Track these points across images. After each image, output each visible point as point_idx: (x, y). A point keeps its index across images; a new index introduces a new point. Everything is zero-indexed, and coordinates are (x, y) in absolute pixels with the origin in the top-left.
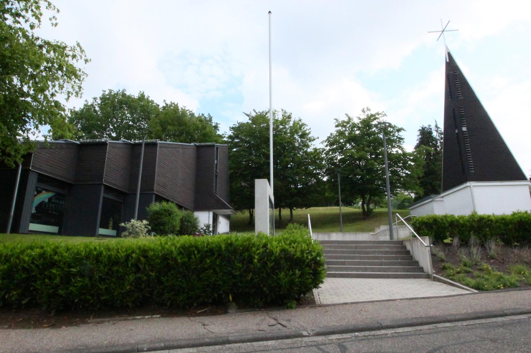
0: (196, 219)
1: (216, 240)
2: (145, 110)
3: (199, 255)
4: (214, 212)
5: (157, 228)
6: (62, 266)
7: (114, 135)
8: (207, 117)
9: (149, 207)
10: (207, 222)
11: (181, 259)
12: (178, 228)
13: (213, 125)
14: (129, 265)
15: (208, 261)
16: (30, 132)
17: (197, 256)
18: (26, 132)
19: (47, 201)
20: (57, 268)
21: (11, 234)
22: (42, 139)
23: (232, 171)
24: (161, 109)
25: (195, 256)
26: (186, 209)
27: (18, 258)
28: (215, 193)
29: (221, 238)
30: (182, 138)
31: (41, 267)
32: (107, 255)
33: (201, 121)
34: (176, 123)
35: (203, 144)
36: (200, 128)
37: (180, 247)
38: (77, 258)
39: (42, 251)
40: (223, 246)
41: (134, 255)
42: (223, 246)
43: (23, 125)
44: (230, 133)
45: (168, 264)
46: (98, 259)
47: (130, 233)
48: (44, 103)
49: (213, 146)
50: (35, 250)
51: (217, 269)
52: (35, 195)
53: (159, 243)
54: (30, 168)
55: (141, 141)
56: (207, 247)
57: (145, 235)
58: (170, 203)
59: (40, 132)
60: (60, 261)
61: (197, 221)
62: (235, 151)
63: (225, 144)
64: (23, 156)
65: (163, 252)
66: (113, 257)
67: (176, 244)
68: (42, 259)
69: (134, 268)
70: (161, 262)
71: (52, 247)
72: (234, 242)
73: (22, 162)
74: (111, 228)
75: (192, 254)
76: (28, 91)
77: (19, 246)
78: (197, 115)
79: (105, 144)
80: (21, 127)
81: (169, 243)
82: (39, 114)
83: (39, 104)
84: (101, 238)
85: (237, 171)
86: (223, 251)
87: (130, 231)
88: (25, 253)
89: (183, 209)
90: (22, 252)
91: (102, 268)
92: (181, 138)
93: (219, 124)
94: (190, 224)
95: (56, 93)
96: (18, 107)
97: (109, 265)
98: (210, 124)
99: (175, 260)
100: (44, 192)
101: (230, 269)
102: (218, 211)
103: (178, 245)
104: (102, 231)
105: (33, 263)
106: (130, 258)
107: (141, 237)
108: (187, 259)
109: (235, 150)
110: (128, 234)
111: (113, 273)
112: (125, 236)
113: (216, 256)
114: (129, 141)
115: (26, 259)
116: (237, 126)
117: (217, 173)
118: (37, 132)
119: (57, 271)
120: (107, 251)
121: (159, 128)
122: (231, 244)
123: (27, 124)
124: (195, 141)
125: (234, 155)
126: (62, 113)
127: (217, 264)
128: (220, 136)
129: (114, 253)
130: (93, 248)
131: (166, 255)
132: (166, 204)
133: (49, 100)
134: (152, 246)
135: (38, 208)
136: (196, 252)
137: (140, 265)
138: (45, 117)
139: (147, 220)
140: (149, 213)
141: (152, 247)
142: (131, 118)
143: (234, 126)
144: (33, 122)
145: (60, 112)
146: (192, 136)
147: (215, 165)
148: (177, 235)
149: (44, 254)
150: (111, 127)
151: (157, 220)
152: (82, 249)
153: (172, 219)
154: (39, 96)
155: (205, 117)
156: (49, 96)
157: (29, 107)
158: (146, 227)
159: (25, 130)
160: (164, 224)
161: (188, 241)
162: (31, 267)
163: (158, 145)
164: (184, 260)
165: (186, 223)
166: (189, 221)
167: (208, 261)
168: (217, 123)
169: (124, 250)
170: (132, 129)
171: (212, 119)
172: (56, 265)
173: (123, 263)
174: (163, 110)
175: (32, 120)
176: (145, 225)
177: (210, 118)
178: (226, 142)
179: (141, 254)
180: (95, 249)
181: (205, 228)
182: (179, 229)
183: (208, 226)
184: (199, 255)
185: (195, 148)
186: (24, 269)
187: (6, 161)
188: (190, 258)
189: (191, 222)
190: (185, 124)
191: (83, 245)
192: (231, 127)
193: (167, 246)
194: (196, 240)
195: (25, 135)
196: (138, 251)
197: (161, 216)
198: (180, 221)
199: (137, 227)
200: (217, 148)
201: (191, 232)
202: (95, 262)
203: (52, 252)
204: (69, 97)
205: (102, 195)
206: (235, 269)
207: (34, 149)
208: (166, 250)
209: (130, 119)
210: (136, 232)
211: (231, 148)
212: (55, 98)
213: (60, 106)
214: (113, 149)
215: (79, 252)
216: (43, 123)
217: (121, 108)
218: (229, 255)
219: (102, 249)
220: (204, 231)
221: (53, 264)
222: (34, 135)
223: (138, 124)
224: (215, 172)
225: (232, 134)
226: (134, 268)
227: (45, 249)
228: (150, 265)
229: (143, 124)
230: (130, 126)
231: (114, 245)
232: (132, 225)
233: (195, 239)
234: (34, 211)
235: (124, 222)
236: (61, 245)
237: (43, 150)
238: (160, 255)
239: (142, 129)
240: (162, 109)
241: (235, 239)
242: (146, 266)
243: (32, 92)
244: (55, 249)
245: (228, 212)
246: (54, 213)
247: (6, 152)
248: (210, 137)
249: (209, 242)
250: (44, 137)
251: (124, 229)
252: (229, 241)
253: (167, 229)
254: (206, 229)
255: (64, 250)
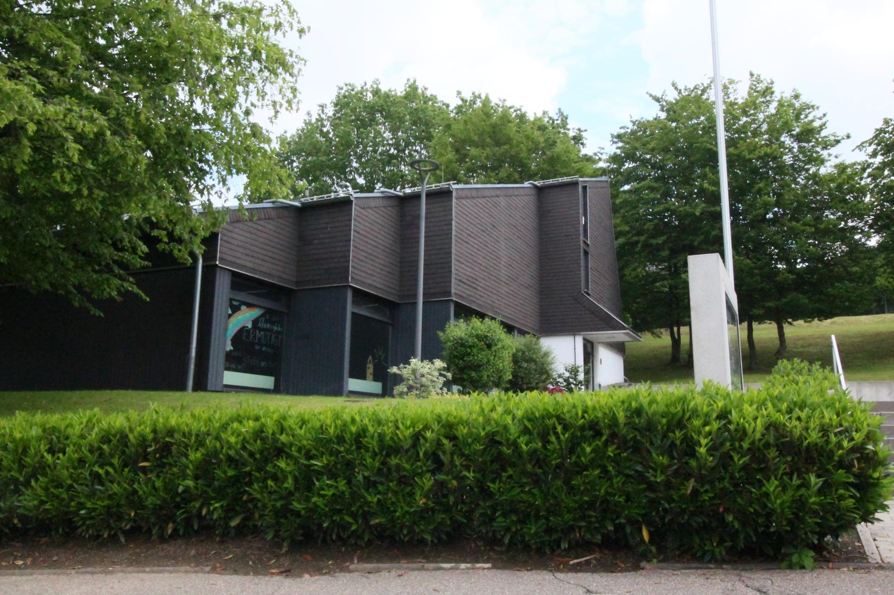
0: (546, 354)
1: (603, 402)
2: (420, 119)
3: (566, 436)
4: (588, 337)
5: (465, 376)
6: (296, 454)
7: (361, 181)
8: (555, 117)
9: (444, 331)
10: (570, 362)
11: (527, 445)
12: (509, 376)
13: (571, 134)
14: (421, 454)
15: (588, 449)
16: (212, 192)
17: (561, 436)
18: (205, 192)
19: (250, 325)
20: (287, 458)
21: (195, 393)
22: (233, 203)
23: (621, 240)
24: (452, 112)
25: (558, 438)
26: (522, 333)
27: (218, 438)
28: (586, 292)
29: (615, 398)
30: (503, 174)
31: (258, 456)
32: (376, 435)
33: (542, 128)
34: (488, 140)
35: (551, 181)
36: (543, 145)
37: (523, 417)
38: (321, 440)
39: (258, 424)
40: (621, 416)
41: (428, 434)
42: (621, 416)
43: (200, 179)
44: (612, 149)
45: (500, 453)
46: (361, 442)
47: (410, 388)
48: (234, 132)
49: (576, 183)
50: (245, 422)
51: (610, 468)
52: (230, 316)
53: (477, 408)
54: (217, 263)
55: (416, 189)
56: (583, 417)
57: (440, 391)
58: (487, 319)
59: (229, 189)
60: (291, 445)
61: (550, 359)
62: (629, 191)
63: (601, 175)
64: (204, 241)
65: (488, 428)
66: (388, 438)
67: (515, 411)
68: (259, 441)
69: (429, 463)
70: (485, 450)
71: (275, 416)
72: (645, 405)
73: (202, 252)
74: (371, 377)
75: (551, 432)
76: (204, 111)
77: (217, 416)
78: (531, 117)
79: (346, 203)
80: (196, 183)
81: (500, 409)
82: (226, 154)
83: (223, 134)
84: (356, 399)
85: (635, 238)
86: (622, 426)
87: (411, 382)
88: (229, 429)
89: (516, 332)
90: (224, 427)
91: (369, 460)
92: (501, 174)
93: (586, 131)
94: (533, 366)
95: (252, 108)
96: (190, 145)
97: (381, 453)
98: (563, 133)
99: (515, 445)
100: (243, 308)
101: (639, 468)
102: (593, 335)
103: (519, 413)
104: (354, 384)
105: (244, 448)
106: (422, 441)
107: (434, 396)
108: (540, 444)
109: (627, 187)
110: (406, 390)
111: (389, 469)
112: (401, 394)
113: (604, 438)
114: (392, 191)
115: (233, 440)
116: (629, 131)
117: (588, 245)
118: (224, 190)
119: (288, 465)
120: (376, 426)
121: (451, 155)
122: (639, 412)
123: (207, 177)
124: (531, 177)
125: (625, 203)
126: (266, 147)
127: (610, 456)
128: (588, 159)
129: (390, 430)
130: (348, 418)
131: (494, 434)
132: (479, 324)
133: (240, 124)
134: (464, 415)
135: (236, 340)
136: (559, 429)
137: (442, 457)
138: (236, 159)
139: (442, 358)
140: (446, 343)
141: (465, 418)
142: (391, 139)
143: (622, 131)
144: (217, 172)
145: (262, 145)
146: (522, 165)
147: (581, 229)
148: (507, 390)
149: (262, 432)
150: (355, 165)
151: (462, 359)
152: (328, 422)
153: (495, 356)
154: (224, 119)
155: (550, 118)
156: (241, 116)
157: (207, 143)
158: (441, 375)
159: (204, 189)
160: (477, 367)
161: (541, 406)
162: (241, 456)
163: (454, 194)
164: (533, 445)
165: (525, 365)
166: (531, 360)
167: (588, 449)
168: (579, 130)
169: (408, 423)
170: (394, 163)
171: (568, 121)
172: (285, 452)
173: (407, 451)
174: (457, 113)
175: (215, 168)
176: (439, 370)
177: (562, 120)
178: (604, 172)
179: (442, 431)
180: (353, 421)
181: (567, 374)
182: (511, 377)
183: (574, 371)
184: (566, 436)
185: (533, 192)
186: (230, 459)
187: (176, 252)
188: (546, 442)
189: (534, 361)
190: (509, 141)
191: (329, 414)
192: (615, 134)
193: (494, 415)
194: (558, 403)
195: (205, 198)
196: (436, 427)
197: (472, 350)
198: (511, 359)
199: (423, 376)
200: (585, 188)
201: (537, 383)
202: (354, 447)
203: (275, 428)
204: (277, 112)
205: (350, 309)
206: (652, 468)
207: (222, 226)
208: (493, 423)
209: (390, 142)
210: (422, 386)
211: (616, 185)
212: (252, 119)
213: (261, 133)
214: (364, 213)
215: (324, 428)
216: (234, 171)
217: (373, 120)
218: (636, 436)
219: (366, 421)
220: (565, 381)
221: (280, 451)
222: (220, 197)
223: (407, 152)
224: (582, 244)
225: (618, 152)
226: (429, 463)
227: (263, 420)
228: (462, 455)
229: (416, 151)
230: (392, 157)
231: (389, 413)
232: (414, 371)
233: (555, 399)
234: (229, 347)
235: (397, 365)
236: (289, 413)
237: (236, 225)
238: (483, 434)
239: (418, 162)
240: (454, 111)
241: (648, 399)
242: (455, 457)
243: (211, 112)
244: (279, 422)
245: (619, 335)
246: (264, 349)
247: (175, 234)
248: (566, 164)
249: (587, 407)
250: (239, 200)
251: (398, 379)
252: (634, 404)
253: (485, 377)
254: (569, 378)
255: (297, 424)
